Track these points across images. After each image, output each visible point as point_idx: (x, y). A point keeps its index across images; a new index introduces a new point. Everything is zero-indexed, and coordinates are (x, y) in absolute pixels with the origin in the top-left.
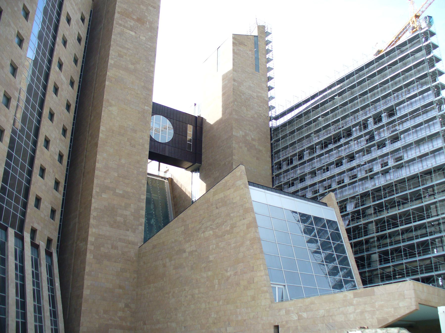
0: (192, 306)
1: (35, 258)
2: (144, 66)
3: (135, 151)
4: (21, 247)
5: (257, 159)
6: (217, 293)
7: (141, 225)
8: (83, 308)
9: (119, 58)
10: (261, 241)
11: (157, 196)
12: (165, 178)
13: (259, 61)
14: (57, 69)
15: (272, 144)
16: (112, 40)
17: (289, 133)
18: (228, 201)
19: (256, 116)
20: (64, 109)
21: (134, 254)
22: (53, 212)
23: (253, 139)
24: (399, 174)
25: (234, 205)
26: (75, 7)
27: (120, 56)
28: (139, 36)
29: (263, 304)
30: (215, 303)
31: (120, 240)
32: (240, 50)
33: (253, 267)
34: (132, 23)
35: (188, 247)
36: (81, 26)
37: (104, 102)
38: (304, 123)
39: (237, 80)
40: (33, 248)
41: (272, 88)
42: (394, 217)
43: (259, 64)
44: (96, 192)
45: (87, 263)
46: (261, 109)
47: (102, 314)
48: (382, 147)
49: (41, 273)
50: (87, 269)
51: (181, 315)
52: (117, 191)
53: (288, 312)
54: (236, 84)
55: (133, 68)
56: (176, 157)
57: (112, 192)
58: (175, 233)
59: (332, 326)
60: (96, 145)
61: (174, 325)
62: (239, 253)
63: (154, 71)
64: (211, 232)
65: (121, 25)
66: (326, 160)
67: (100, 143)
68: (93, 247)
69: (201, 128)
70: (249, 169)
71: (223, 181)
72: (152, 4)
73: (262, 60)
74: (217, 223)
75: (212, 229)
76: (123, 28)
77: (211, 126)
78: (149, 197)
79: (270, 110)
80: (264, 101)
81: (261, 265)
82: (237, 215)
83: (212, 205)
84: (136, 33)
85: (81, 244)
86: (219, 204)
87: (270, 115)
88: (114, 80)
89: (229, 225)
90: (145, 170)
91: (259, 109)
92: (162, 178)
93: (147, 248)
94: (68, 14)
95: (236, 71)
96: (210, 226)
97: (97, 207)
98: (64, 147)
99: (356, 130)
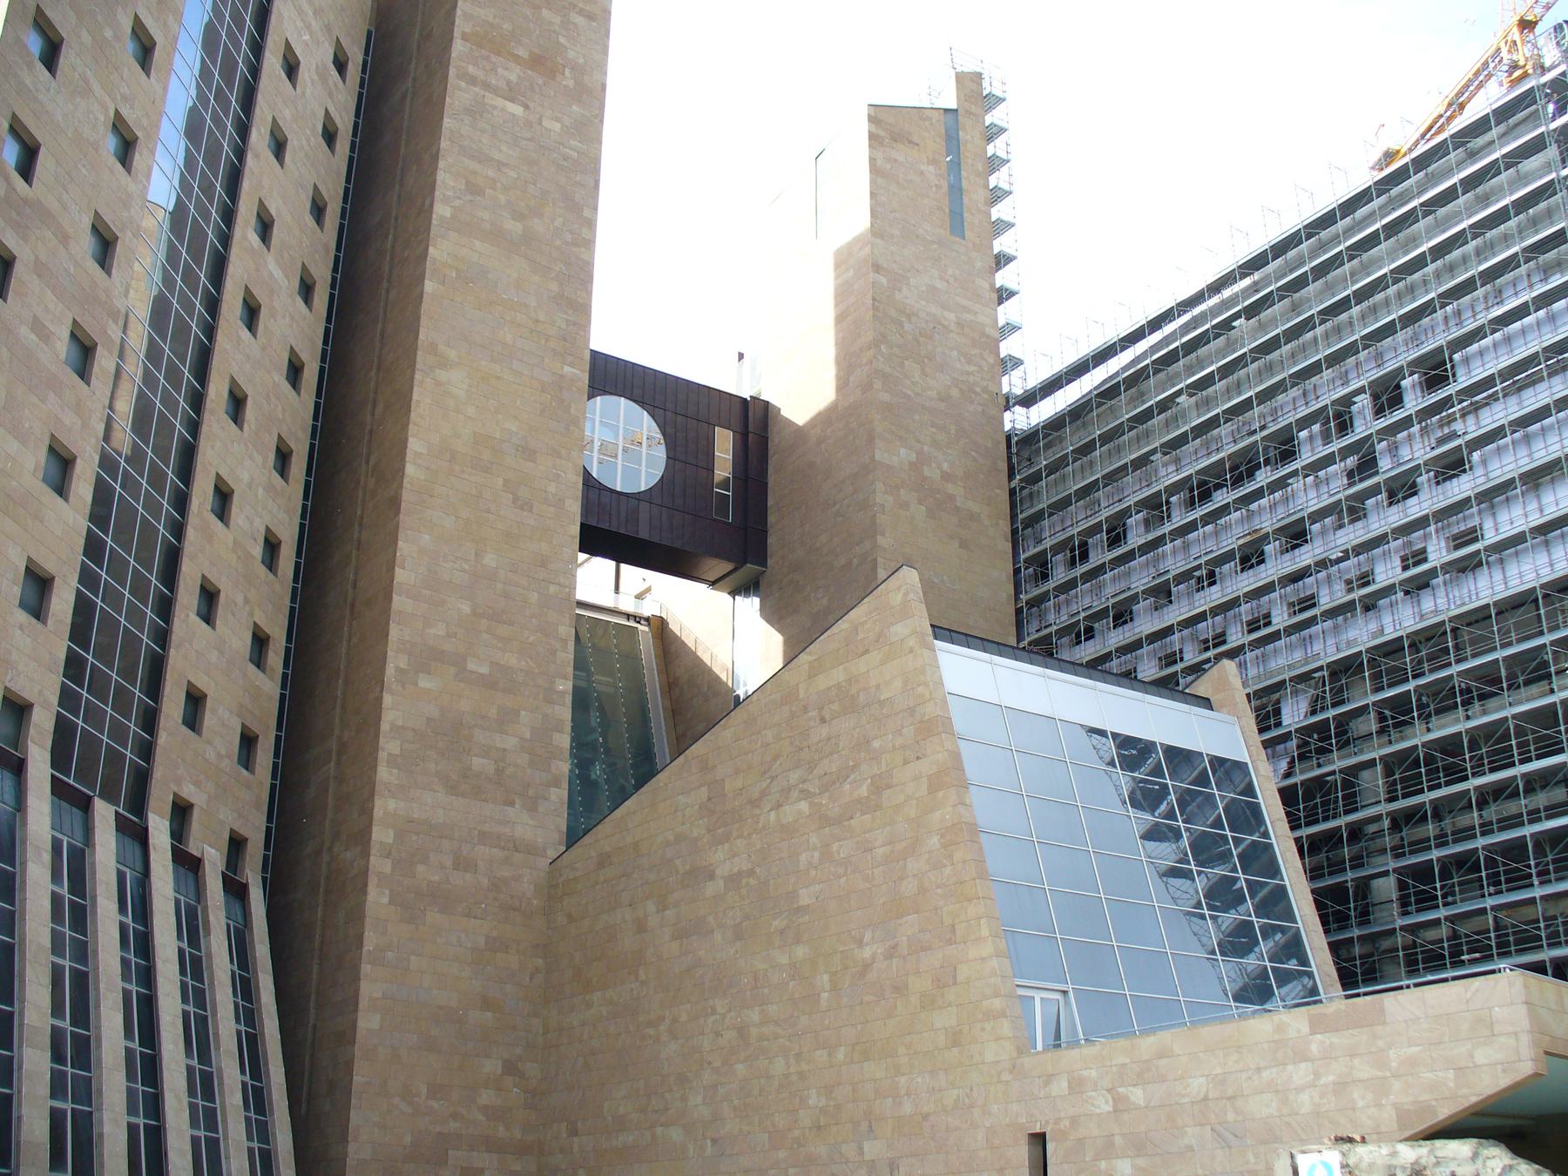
0: (740, 1069)
1: (188, 905)
2: (556, 224)
3: (532, 522)
4: (139, 866)
5: (964, 544)
6: (827, 1022)
7: (557, 784)
8: (357, 1079)
9: (468, 197)
10: (981, 834)
11: (610, 680)
12: (637, 618)
13: (962, 199)
14: (254, 239)
15: (1012, 492)
16: (445, 132)
17: (1072, 451)
18: (862, 698)
19: (955, 393)
20: (280, 379)
21: (532, 887)
22: (248, 741)
23: (947, 477)
24: (1465, 591)
25: (884, 711)
26: (313, 23)
27: (474, 189)
28: (538, 116)
29: (989, 1057)
30: (821, 1056)
31: (484, 837)
32: (896, 160)
33: (953, 926)
34: (514, 74)
35: (723, 861)
36: (336, 85)
37: (419, 353)
38: (1127, 417)
39: (885, 266)
40: (182, 870)
41: (1011, 294)
42: (1450, 746)
43: (965, 210)
44: (398, 669)
45: (368, 920)
46: (976, 368)
47: (424, 1097)
48: (1405, 498)
49: (209, 956)
50: (371, 940)
51: (699, 1099)
52: (471, 666)
53: (1077, 1086)
54: (884, 280)
55: (520, 232)
56: (678, 545)
57: (452, 670)
58: (676, 811)
59: (1236, 1136)
60: (395, 504)
61: (676, 1134)
62: (901, 879)
63: (594, 242)
64: (804, 806)
65: (473, 81)
66: (1206, 545)
67: (407, 496)
68: (389, 862)
69: (764, 440)
70: (936, 581)
71: (843, 625)
73: (974, 196)
74: (825, 774)
75: (806, 794)
76: (483, 92)
77: (799, 432)
78: (583, 684)
79: (1005, 372)
80: (983, 340)
81: (983, 921)
82: (894, 747)
83: (805, 710)
84: (526, 107)
85: (349, 855)
86: (830, 706)
87: (1005, 389)
88: (454, 275)
89: (866, 779)
90: (567, 590)
92: (628, 616)
93: (578, 865)
94: (288, 44)
95: (882, 237)
96: (801, 786)
97: (400, 723)
98: (282, 516)
99: (1311, 438)
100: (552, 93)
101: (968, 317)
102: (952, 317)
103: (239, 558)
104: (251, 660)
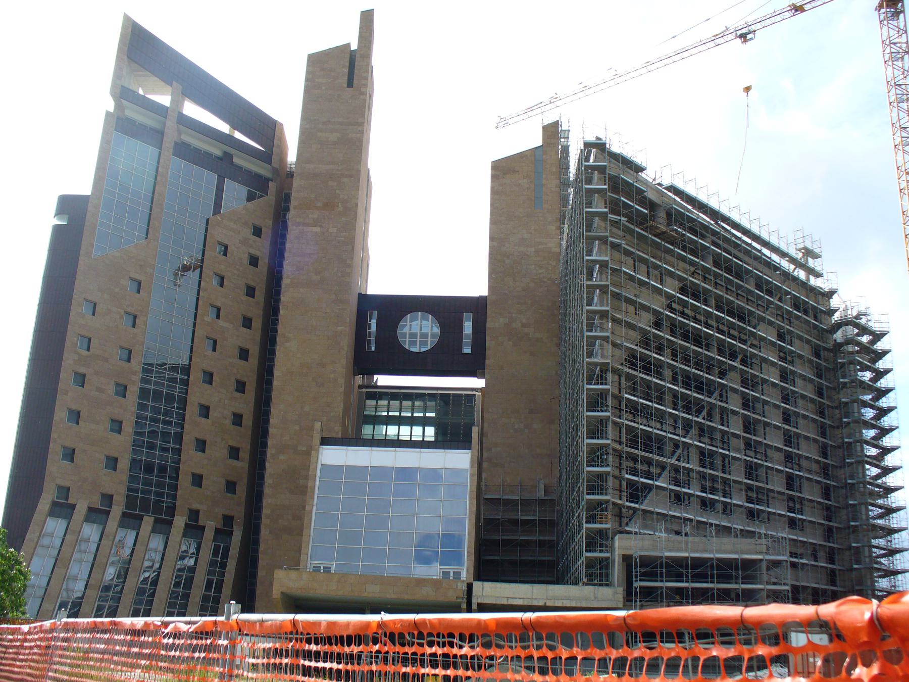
23: (524, 325)
32: (505, 184)
34: (315, 215)
44: (271, 454)
50: (262, 547)
52: (300, 448)
54: (495, 244)
72: (346, 173)
84: (321, 226)
91: (540, 271)
100: (333, 216)
101: (541, 247)
102: (533, 249)
103: (216, 427)
104: (231, 457)
